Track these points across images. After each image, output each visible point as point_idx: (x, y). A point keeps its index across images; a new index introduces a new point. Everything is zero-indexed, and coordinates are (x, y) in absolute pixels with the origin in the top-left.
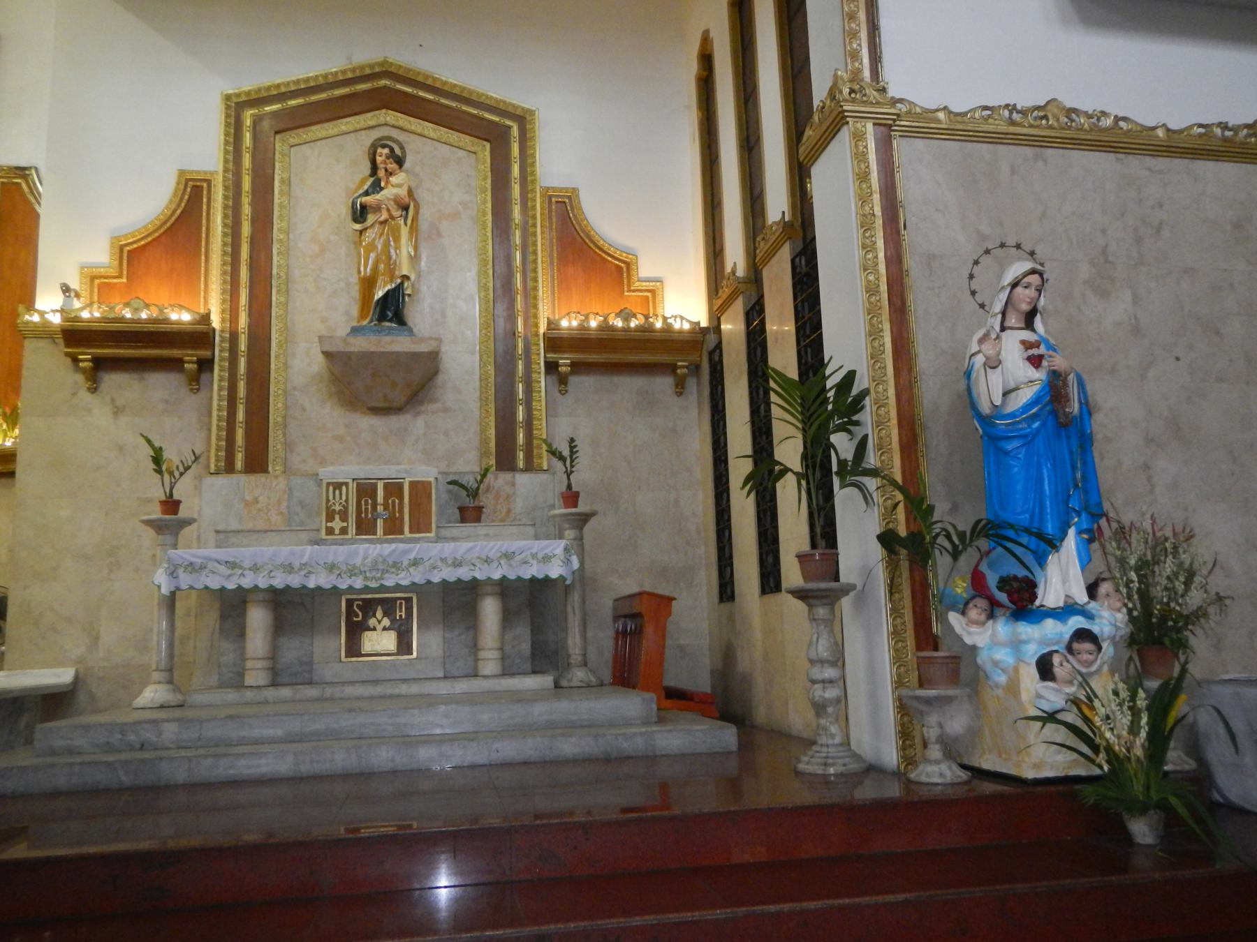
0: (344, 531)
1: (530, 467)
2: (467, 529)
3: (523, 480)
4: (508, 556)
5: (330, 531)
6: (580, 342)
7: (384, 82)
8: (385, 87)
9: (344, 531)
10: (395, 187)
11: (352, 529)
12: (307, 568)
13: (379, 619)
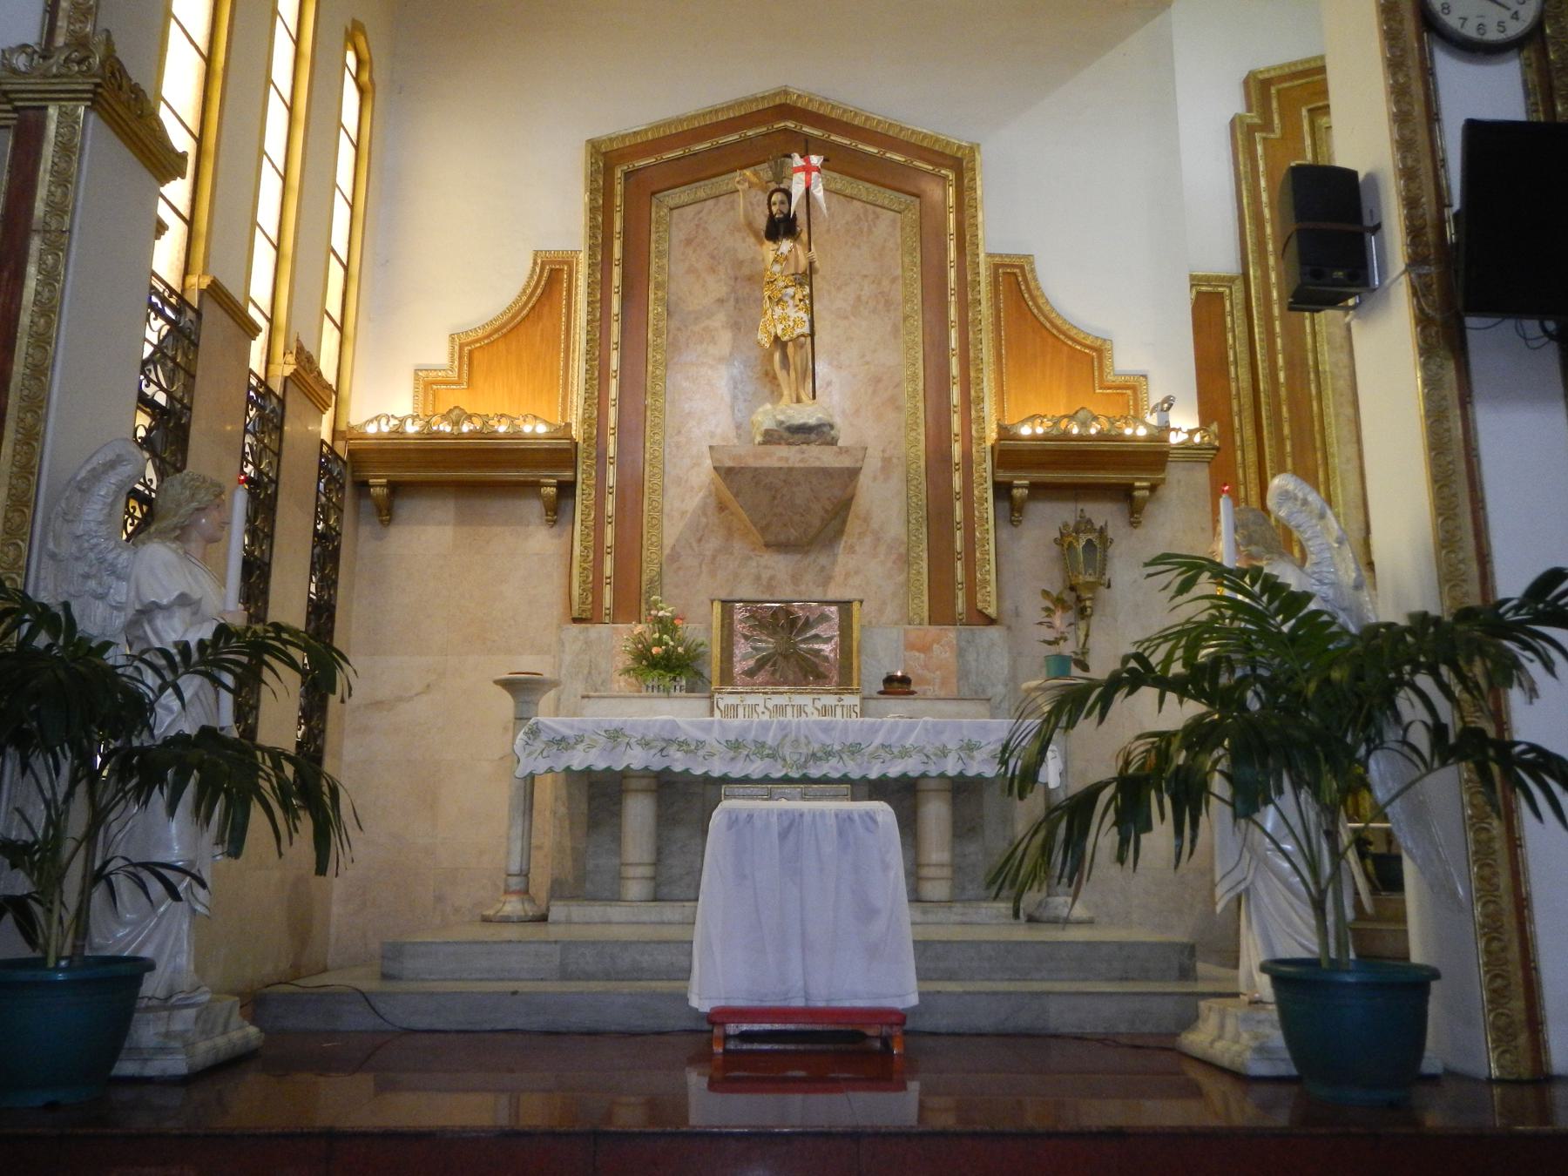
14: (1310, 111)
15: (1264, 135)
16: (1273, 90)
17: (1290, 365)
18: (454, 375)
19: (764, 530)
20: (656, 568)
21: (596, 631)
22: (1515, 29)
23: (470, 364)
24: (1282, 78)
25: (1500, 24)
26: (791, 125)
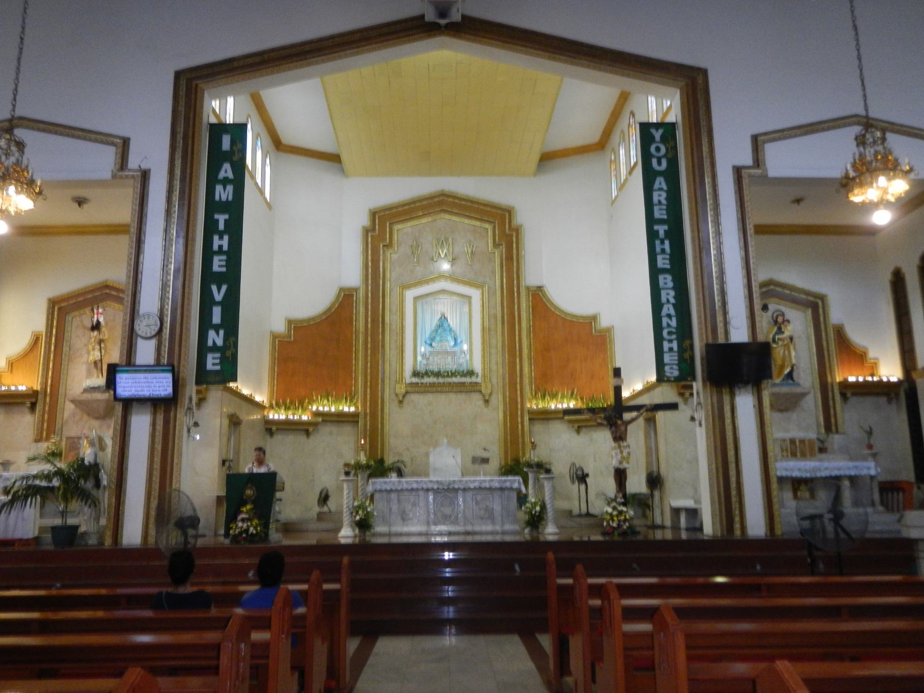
0: (787, 456)
1: (837, 432)
2: (823, 456)
3: (836, 437)
4: (856, 467)
5: (783, 456)
6: (856, 385)
7: (772, 287)
8: (772, 289)
9: (787, 456)
10: (788, 331)
11: (790, 456)
12: (792, 470)
13: (803, 487)
14: (389, 224)
15: (372, 234)
16: (377, 216)
17: (373, 321)
18: (6, 370)
19: (89, 415)
20: (60, 426)
21: (40, 444)
22: (153, 333)
23: (12, 366)
24: (380, 211)
25: (151, 333)
26: (108, 291)
